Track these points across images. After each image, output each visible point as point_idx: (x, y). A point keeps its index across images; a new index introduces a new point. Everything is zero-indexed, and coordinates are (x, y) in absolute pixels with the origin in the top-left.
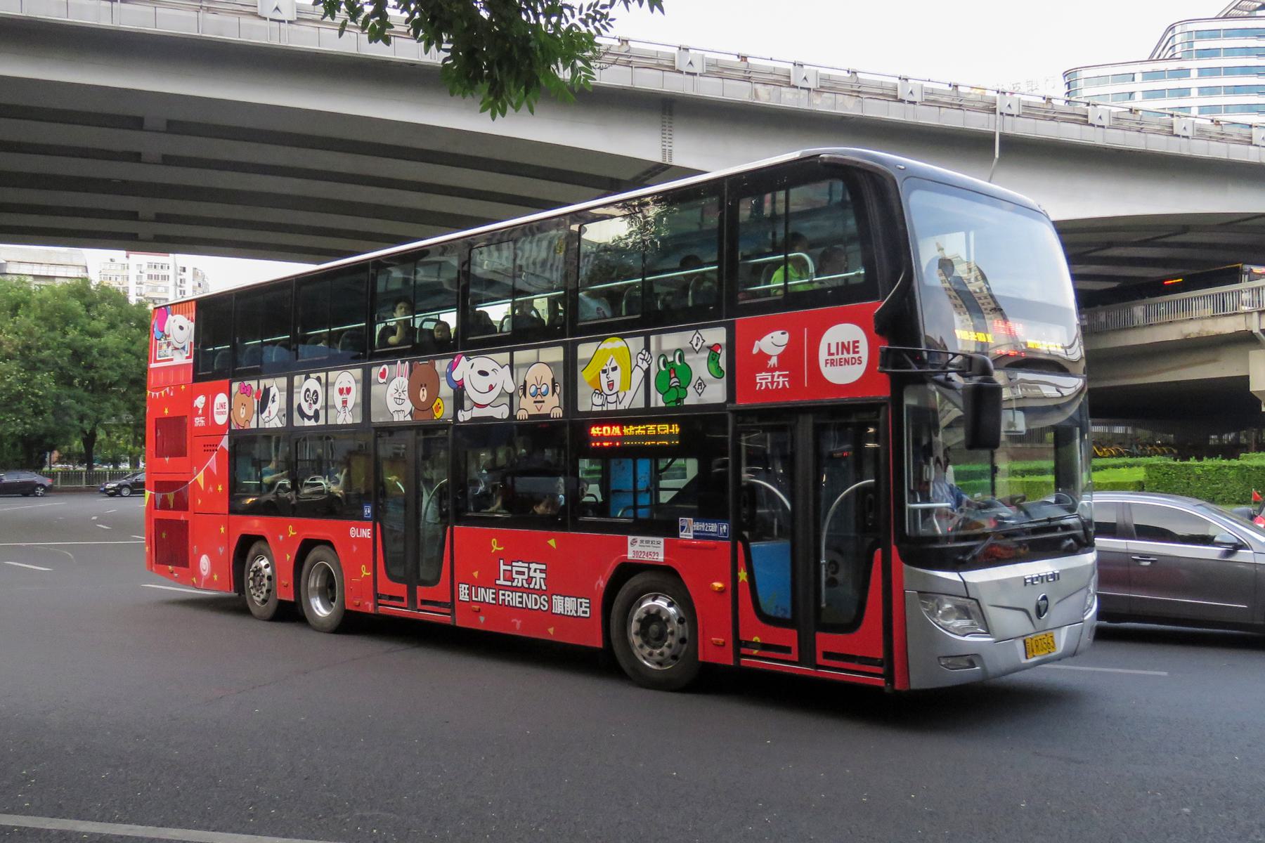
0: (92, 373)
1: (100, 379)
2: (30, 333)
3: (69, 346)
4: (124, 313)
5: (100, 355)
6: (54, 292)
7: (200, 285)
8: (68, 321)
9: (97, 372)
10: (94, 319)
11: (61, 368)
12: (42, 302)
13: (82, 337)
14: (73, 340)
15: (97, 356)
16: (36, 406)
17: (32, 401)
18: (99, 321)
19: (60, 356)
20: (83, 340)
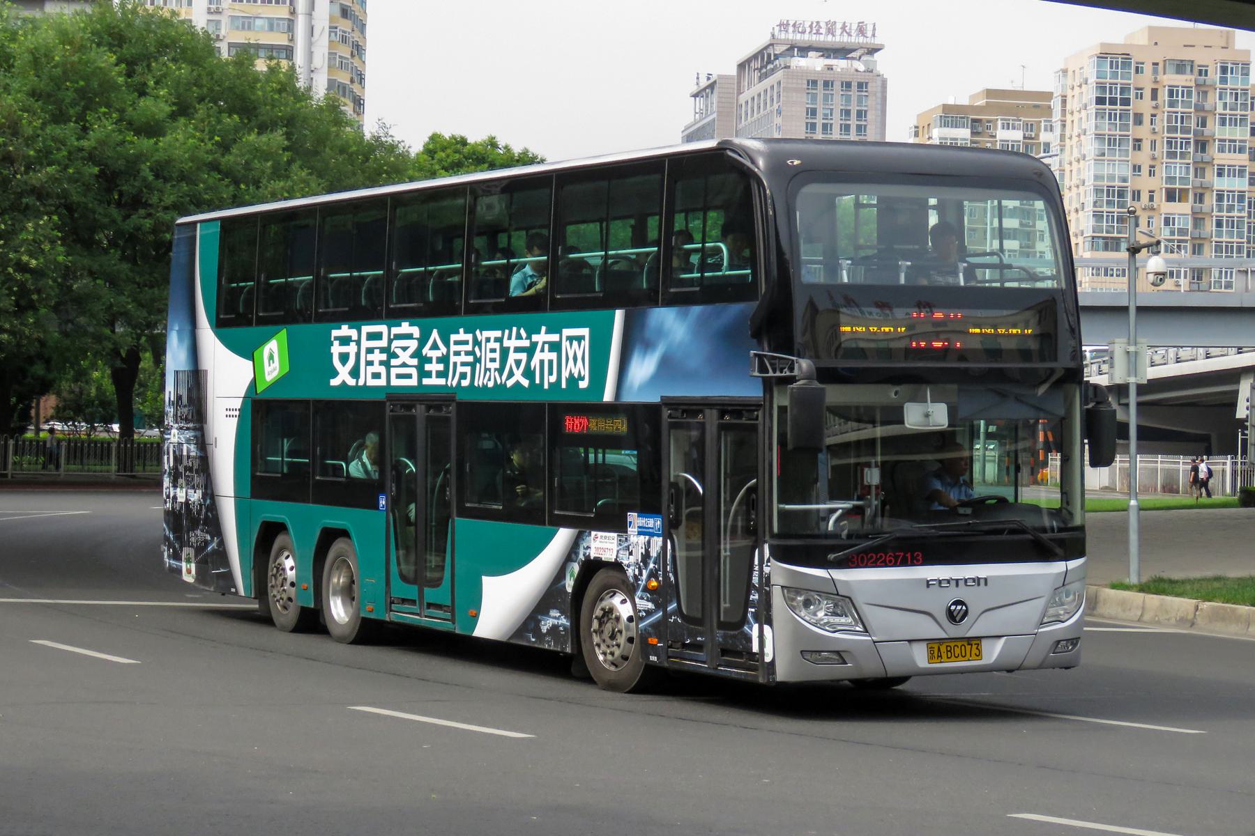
1: (154, 231)
2: (14, 129)
3: (91, 158)
4: (205, 81)
5: (157, 176)
6: (65, 37)
7: (345, 12)
8: (91, 100)
9: (149, 215)
10: (142, 94)
11: (70, 208)
12: (38, 59)
14: (102, 143)
15: (151, 178)
16: (23, 291)
17: (17, 280)
20: (123, 142)
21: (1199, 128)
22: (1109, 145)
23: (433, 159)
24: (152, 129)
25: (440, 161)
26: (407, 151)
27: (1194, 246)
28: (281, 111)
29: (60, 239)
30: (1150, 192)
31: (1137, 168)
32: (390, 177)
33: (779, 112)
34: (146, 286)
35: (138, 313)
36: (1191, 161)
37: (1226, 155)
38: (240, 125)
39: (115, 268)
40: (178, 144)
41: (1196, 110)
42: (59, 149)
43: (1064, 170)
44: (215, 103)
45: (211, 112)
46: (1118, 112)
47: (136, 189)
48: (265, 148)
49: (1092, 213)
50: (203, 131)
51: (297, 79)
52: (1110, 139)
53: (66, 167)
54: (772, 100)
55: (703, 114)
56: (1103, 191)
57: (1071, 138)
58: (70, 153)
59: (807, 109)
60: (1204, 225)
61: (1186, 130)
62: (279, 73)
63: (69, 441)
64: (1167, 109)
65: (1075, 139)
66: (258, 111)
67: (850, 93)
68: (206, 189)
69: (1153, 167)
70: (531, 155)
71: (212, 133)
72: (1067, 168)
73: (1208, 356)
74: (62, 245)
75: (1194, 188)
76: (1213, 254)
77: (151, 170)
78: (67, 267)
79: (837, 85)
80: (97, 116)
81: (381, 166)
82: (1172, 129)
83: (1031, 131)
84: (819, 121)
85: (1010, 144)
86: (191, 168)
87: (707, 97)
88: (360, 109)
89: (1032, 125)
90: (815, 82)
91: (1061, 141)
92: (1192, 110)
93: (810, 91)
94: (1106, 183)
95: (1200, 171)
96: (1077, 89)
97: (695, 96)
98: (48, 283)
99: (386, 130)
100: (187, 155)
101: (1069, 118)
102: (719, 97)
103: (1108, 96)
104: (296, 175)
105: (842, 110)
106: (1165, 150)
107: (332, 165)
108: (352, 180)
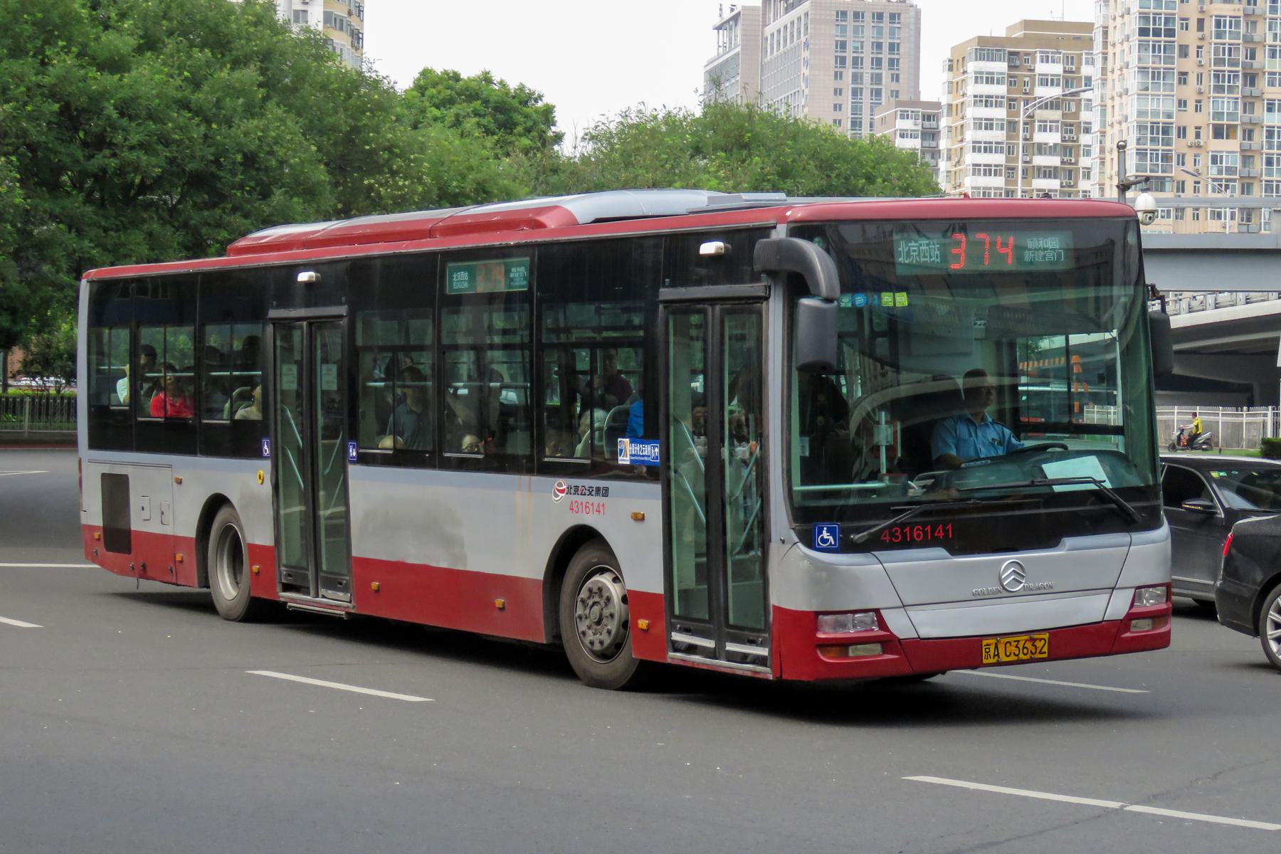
0: (103, 159)
1: (121, 171)
3: (53, 95)
4: (175, 12)
5: (122, 114)
8: (51, 32)
9: (114, 155)
10: (107, 27)
11: (32, 147)
13: (82, 72)
14: (63, 79)
15: (115, 115)
18: (119, 30)
19: (30, 118)
20: (84, 79)
21: (1248, 60)
22: (1153, 78)
23: (423, 95)
24: (115, 65)
25: (432, 97)
26: (392, 88)
27: (1243, 185)
28: (256, 45)
29: (19, 181)
30: (1196, 128)
31: (1182, 104)
32: (374, 116)
33: (807, 45)
34: (112, 230)
35: (104, 258)
36: (1240, 96)
37: (1277, 89)
38: (213, 60)
39: (78, 211)
40: (144, 80)
41: (1245, 41)
42: (18, 86)
43: (1106, 106)
44: (186, 39)
45: (181, 46)
46: (1163, 44)
47: (99, 128)
48: (237, 85)
49: (1135, 151)
50: (172, 67)
51: (275, 11)
52: (1153, 73)
53: (25, 104)
54: (799, 32)
55: (726, 47)
56: (1146, 127)
57: (1113, 71)
58: (29, 89)
59: (837, 41)
60: (1253, 163)
61: (1234, 63)
62: (255, 4)
63: (33, 398)
64: (1214, 40)
65: (1117, 72)
66: (232, 45)
67: (881, 25)
68: (173, 129)
69: (1199, 101)
70: (527, 91)
71: (181, 68)
72: (1109, 103)
73: (1248, 301)
74: (21, 187)
75: (1243, 124)
76: (1263, 194)
77: (116, 108)
78: (27, 211)
79: (868, 17)
80: (56, 50)
81: (365, 104)
82: (1219, 62)
83: (1072, 64)
84: (849, 55)
85: (1050, 78)
86: (159, 105)
87: (731, 29)
88: (358, 43)
89: (1072, 58)
90: (844, 14)
91: (1102, 74)
92: (1241, 41)
93: (839, 23)
94: (1149, 119)
95: (1249, 105)
96: (1119, 19)
97: (719, 28)
98: (5, 228)
99: (370, 65)
100: (154, 92)
101: (1110, 50)
102: (743, 30)
103: (1151, 27)
104: (272, 113)
105: (873, 43)
106: (1212, 84)
107: (310, 103)
108: (334, 118)
